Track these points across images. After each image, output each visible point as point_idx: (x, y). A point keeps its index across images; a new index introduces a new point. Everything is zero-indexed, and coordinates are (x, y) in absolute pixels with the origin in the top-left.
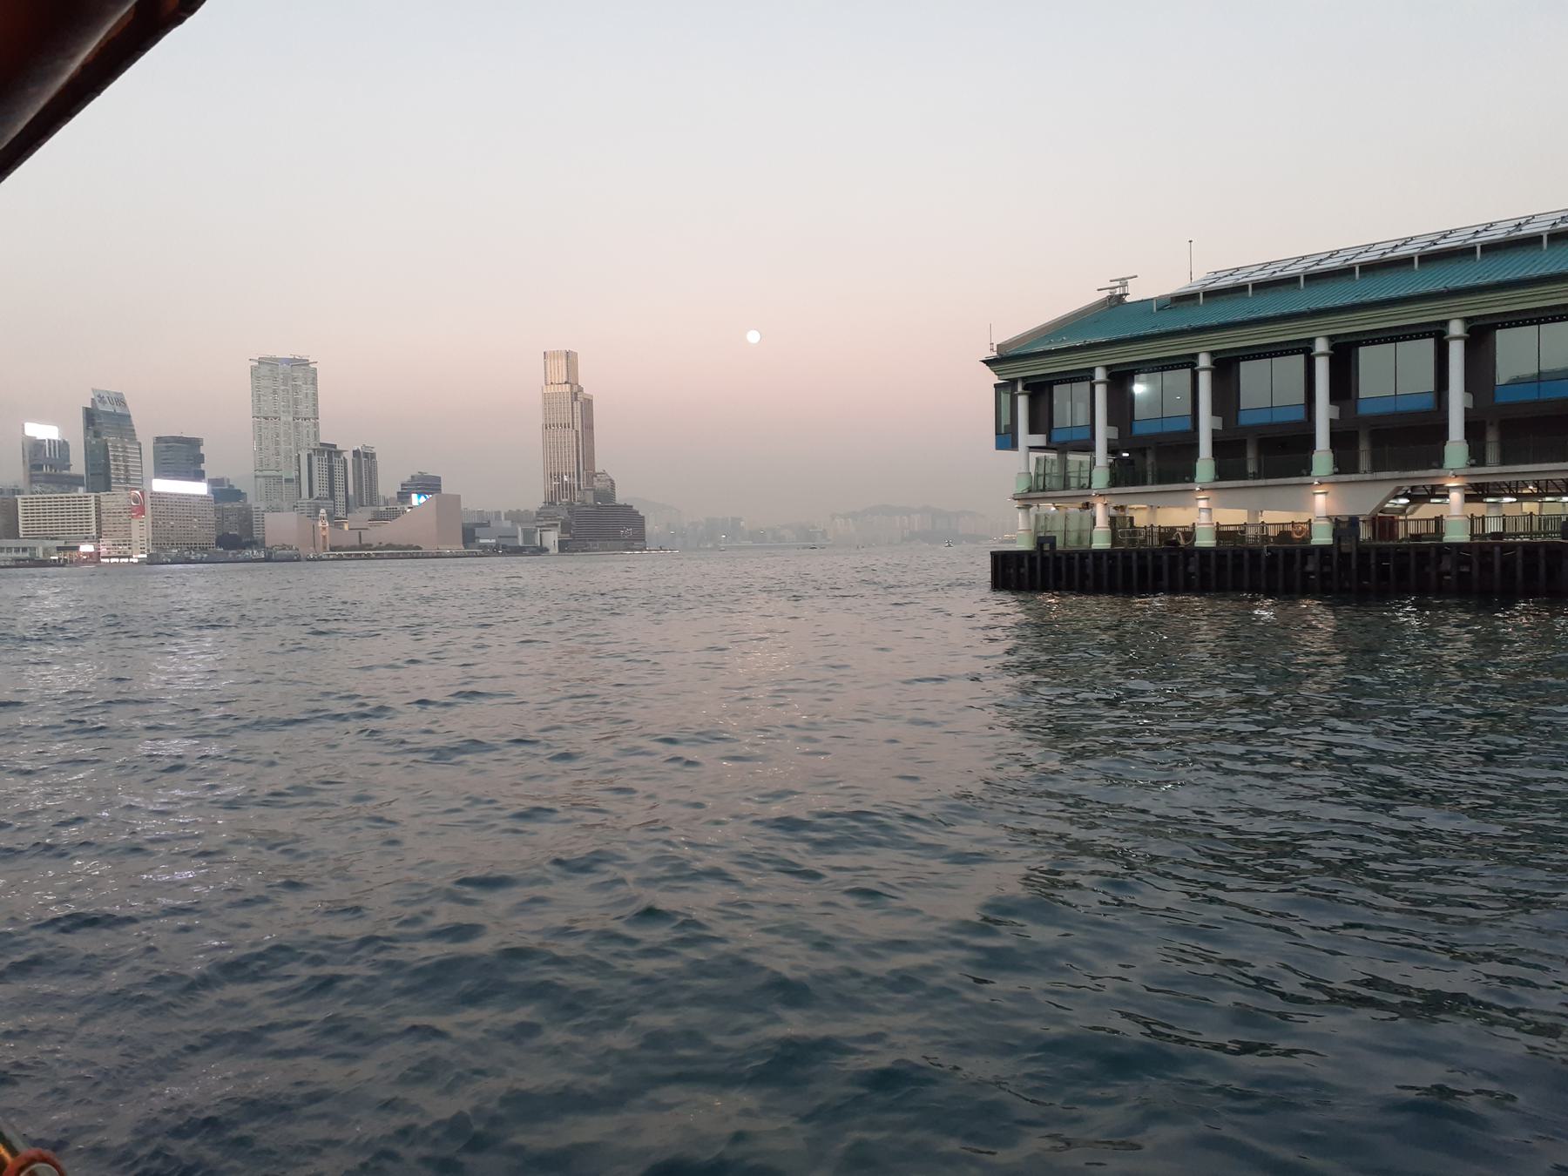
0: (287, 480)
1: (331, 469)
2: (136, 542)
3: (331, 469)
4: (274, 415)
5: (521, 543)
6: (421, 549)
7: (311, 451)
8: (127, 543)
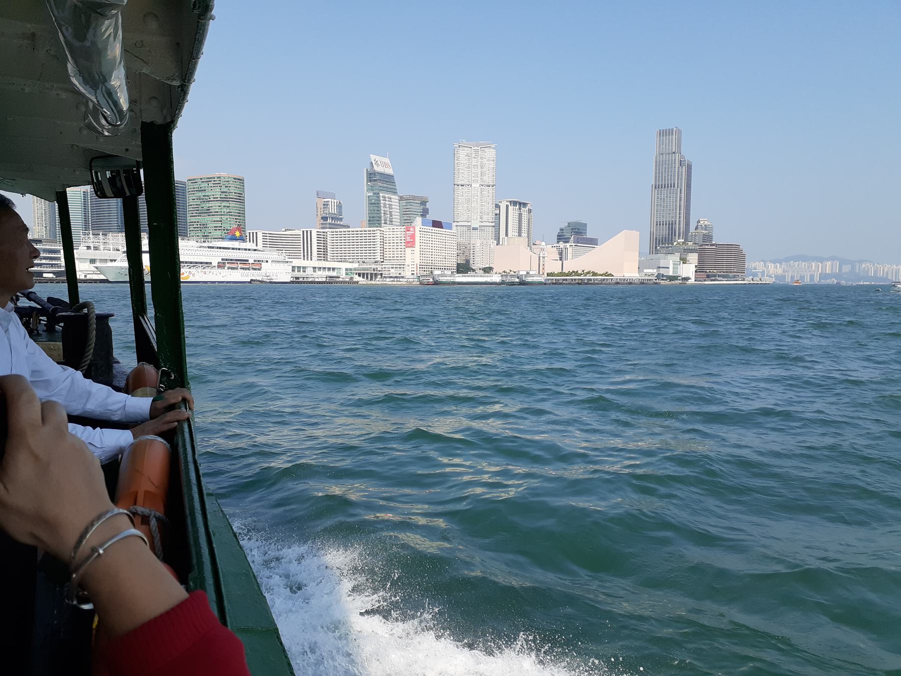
0: (474, 229)
1: (520, 215)
2: (409, 266)
3: (520, 215)
4: (468, 183)
5: (671, 274)
6: (613, 276)
7: (509, 203)
8: (402, 266)
